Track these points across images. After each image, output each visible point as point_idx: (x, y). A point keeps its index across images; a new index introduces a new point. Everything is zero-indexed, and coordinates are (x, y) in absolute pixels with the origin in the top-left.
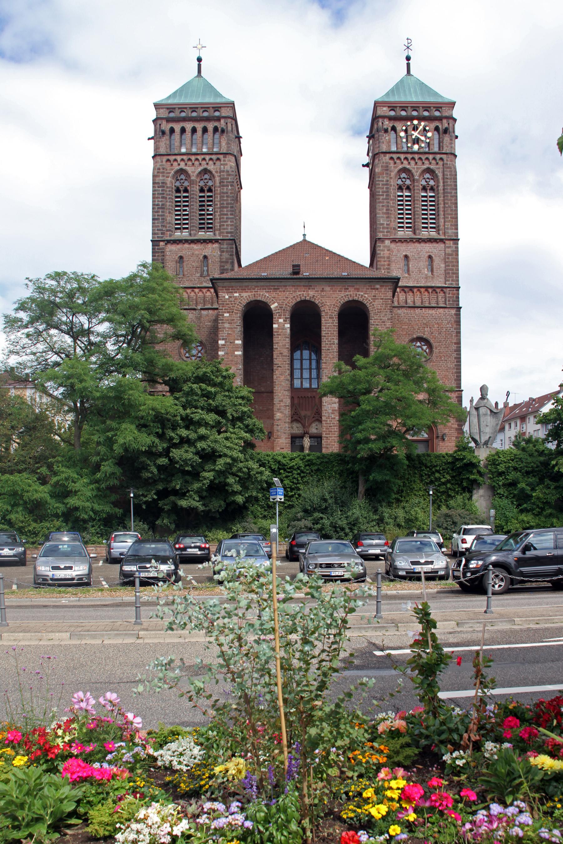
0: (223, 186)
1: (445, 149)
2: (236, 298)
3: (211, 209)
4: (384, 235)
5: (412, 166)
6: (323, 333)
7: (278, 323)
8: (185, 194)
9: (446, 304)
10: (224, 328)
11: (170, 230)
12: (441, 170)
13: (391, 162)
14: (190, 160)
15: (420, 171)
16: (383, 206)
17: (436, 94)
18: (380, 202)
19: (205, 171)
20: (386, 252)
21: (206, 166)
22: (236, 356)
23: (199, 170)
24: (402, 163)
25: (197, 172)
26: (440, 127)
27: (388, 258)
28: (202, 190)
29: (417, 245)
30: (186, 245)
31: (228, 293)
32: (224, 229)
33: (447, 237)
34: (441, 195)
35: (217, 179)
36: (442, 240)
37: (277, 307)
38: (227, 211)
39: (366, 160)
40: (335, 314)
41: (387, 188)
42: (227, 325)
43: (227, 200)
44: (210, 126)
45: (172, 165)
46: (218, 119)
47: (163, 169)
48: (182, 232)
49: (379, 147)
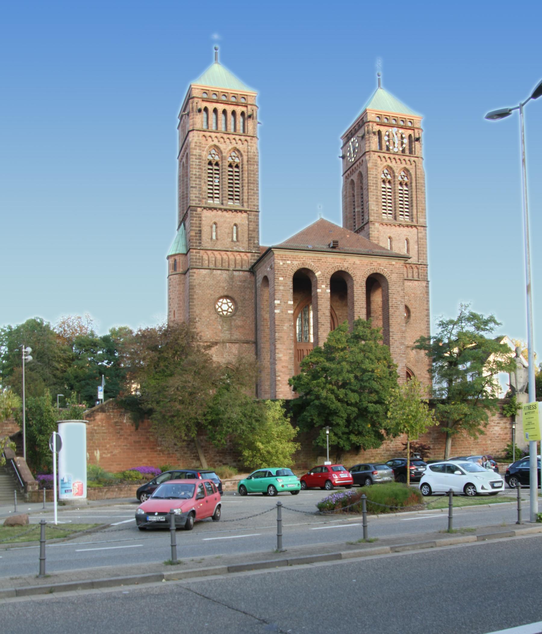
0: (251, 164)
1: (416, 153)
2: (288, 265)
3: (217, 180)
4: (374, 219)
5: (393, 164)
6: (355, 299)
7: (321, 288)
8: (217, 168)
9: (419, 278)
10: (280, 290)
11: (205, 198)
15: (399, 169)
16: (373, 195)
18: (371, 192)
20: (376, 232)
21: (235, 145)
22: (289, 314)
23: (230, 148)
24: (386, 161)
25: (228, 149)
26: (413, 135)
27: (378, 238)
28: (230, 166)
30: (220, 212)
31: (282, 260)
32: (252, 202)
33: (419, 224)
34: (414, 190)
35: (245, 158)
37: (320, 275)
38: (254, 187)
40: (364, 284)
41: (376, 181)
42: (281, 288)
43: (253, 177)
45: (207, 140)
47: (200, 143)
48: (213, 200)
49: (369, 146)
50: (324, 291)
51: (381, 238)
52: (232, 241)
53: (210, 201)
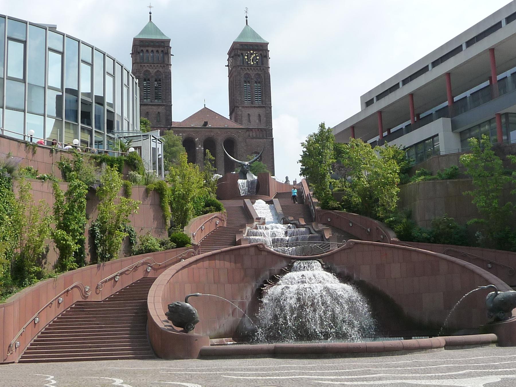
14: (151, 66)
17: (261, 38)
19: (158, 71)
29: (253, 109)
30: (150, 107)
39: (227, 64)
44: (160, 49)
53: (145, 101)
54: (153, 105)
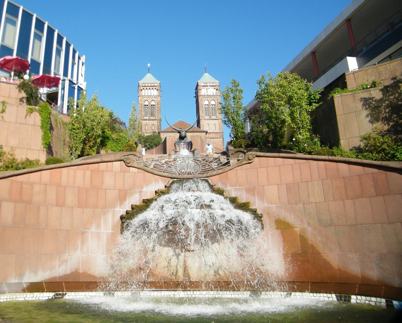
12: (216, 100)
13: (203, 98)
30: (148, 121)
36: (217, 119)
44: (154, 88)
46: (156, 86)
50: (266, 154)
51: (204, 125)
52: (152, 129)
53: (145, 117)
54: (150, 120)
